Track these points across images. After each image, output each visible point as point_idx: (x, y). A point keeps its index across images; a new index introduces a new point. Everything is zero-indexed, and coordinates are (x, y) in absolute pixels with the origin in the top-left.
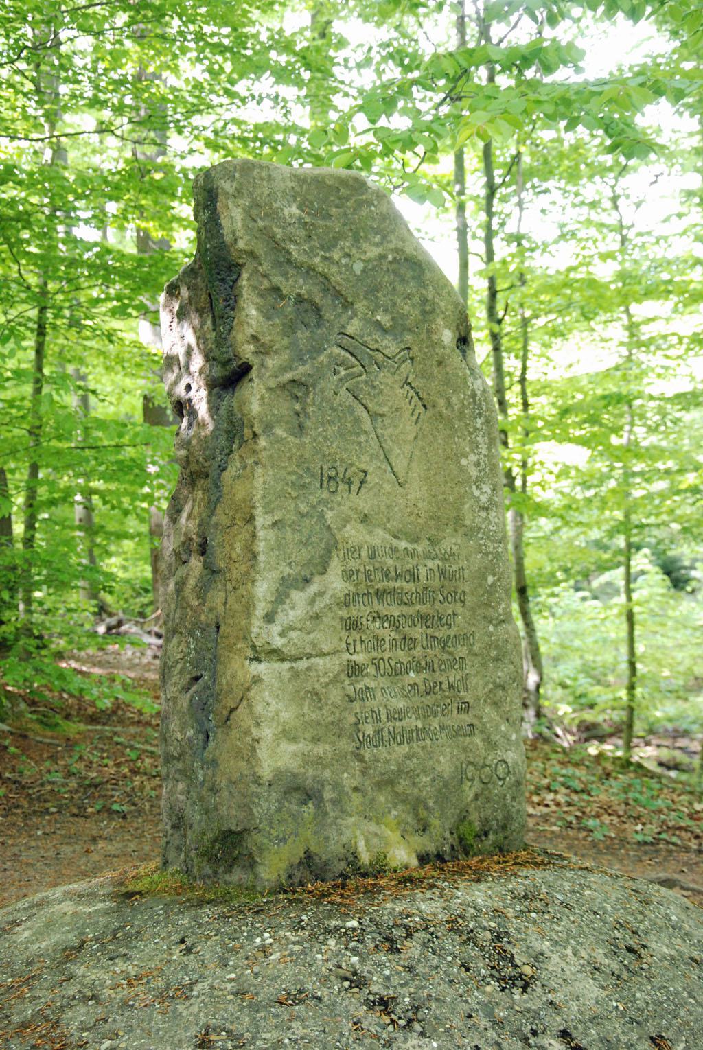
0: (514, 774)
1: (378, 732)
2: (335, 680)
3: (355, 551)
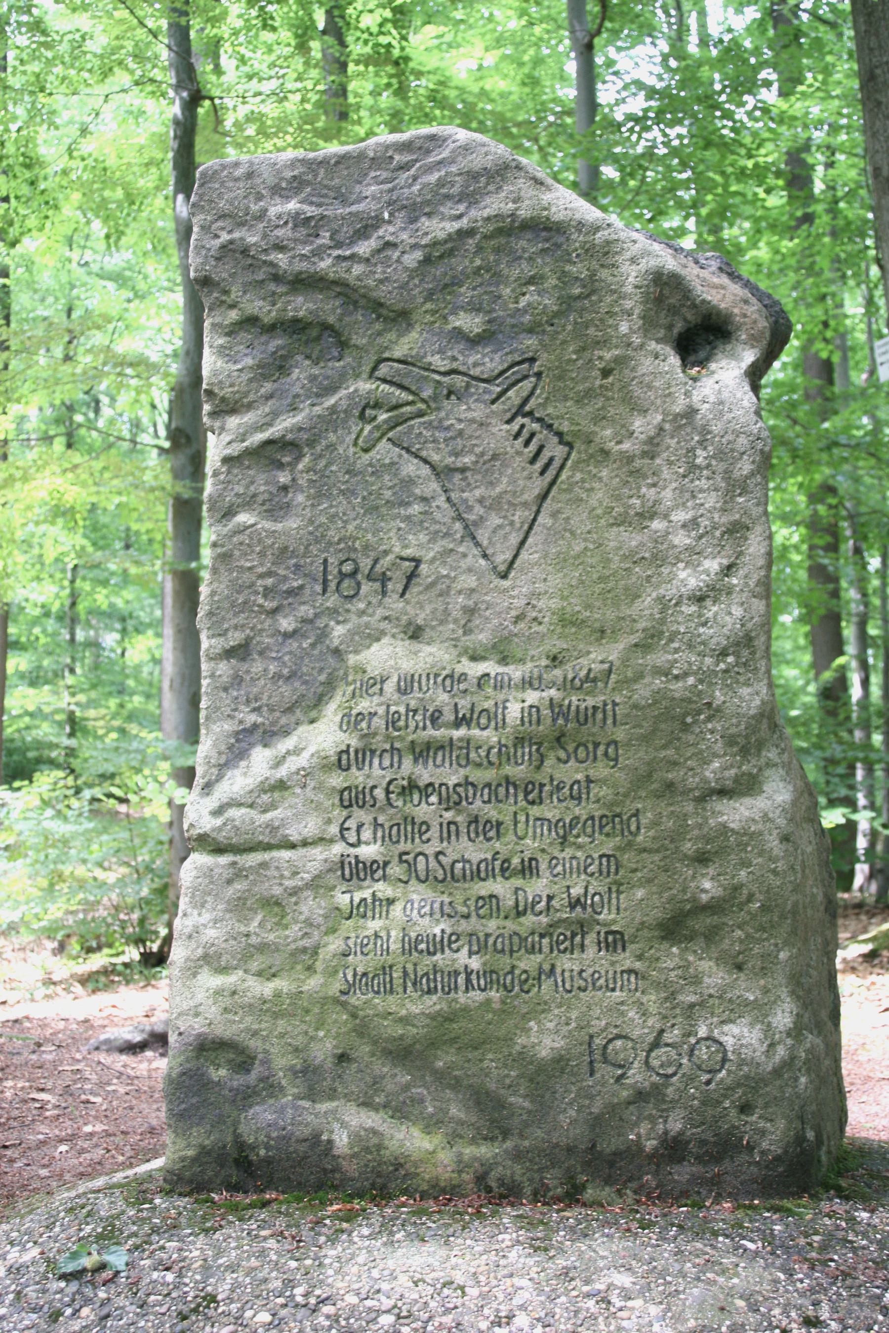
2: (316, 884)
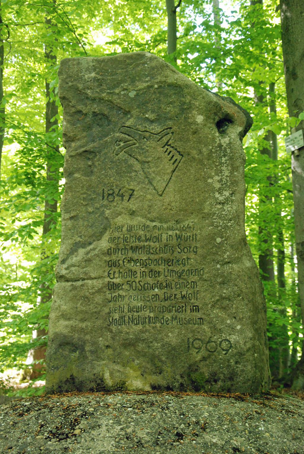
0: (236, 348)
1: (122, 317)
2: (99, 291)
3: (119, 228)
